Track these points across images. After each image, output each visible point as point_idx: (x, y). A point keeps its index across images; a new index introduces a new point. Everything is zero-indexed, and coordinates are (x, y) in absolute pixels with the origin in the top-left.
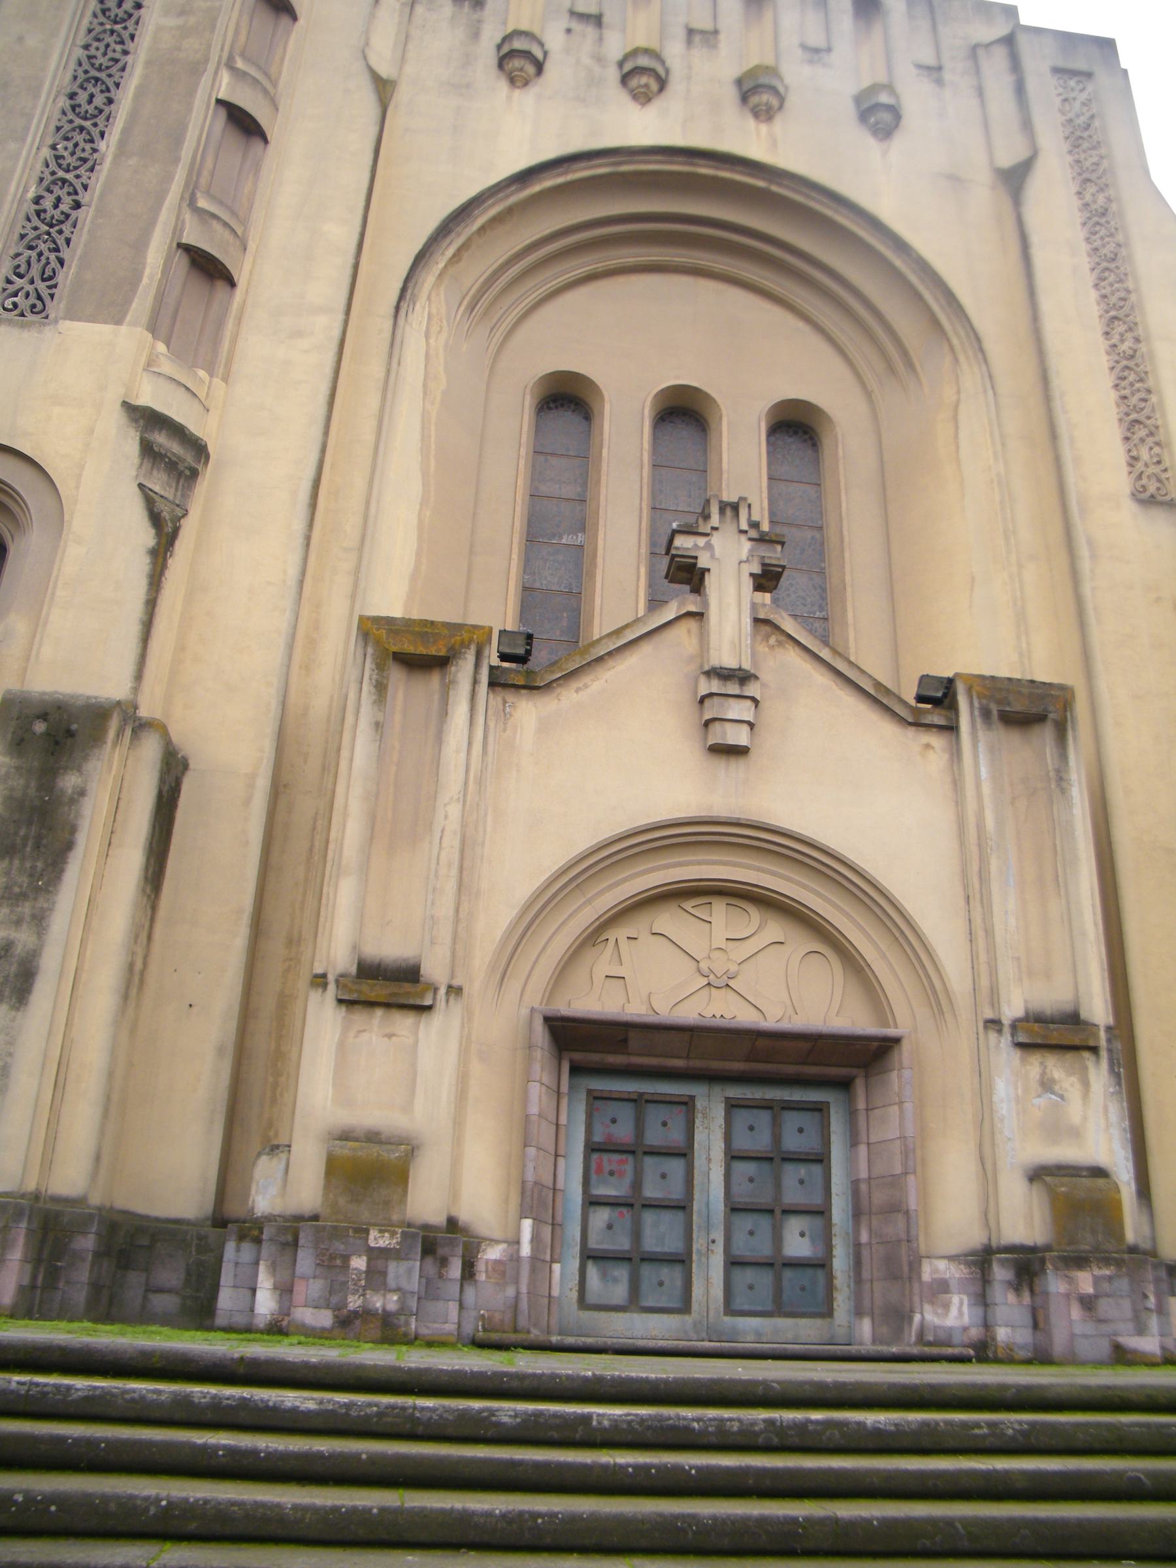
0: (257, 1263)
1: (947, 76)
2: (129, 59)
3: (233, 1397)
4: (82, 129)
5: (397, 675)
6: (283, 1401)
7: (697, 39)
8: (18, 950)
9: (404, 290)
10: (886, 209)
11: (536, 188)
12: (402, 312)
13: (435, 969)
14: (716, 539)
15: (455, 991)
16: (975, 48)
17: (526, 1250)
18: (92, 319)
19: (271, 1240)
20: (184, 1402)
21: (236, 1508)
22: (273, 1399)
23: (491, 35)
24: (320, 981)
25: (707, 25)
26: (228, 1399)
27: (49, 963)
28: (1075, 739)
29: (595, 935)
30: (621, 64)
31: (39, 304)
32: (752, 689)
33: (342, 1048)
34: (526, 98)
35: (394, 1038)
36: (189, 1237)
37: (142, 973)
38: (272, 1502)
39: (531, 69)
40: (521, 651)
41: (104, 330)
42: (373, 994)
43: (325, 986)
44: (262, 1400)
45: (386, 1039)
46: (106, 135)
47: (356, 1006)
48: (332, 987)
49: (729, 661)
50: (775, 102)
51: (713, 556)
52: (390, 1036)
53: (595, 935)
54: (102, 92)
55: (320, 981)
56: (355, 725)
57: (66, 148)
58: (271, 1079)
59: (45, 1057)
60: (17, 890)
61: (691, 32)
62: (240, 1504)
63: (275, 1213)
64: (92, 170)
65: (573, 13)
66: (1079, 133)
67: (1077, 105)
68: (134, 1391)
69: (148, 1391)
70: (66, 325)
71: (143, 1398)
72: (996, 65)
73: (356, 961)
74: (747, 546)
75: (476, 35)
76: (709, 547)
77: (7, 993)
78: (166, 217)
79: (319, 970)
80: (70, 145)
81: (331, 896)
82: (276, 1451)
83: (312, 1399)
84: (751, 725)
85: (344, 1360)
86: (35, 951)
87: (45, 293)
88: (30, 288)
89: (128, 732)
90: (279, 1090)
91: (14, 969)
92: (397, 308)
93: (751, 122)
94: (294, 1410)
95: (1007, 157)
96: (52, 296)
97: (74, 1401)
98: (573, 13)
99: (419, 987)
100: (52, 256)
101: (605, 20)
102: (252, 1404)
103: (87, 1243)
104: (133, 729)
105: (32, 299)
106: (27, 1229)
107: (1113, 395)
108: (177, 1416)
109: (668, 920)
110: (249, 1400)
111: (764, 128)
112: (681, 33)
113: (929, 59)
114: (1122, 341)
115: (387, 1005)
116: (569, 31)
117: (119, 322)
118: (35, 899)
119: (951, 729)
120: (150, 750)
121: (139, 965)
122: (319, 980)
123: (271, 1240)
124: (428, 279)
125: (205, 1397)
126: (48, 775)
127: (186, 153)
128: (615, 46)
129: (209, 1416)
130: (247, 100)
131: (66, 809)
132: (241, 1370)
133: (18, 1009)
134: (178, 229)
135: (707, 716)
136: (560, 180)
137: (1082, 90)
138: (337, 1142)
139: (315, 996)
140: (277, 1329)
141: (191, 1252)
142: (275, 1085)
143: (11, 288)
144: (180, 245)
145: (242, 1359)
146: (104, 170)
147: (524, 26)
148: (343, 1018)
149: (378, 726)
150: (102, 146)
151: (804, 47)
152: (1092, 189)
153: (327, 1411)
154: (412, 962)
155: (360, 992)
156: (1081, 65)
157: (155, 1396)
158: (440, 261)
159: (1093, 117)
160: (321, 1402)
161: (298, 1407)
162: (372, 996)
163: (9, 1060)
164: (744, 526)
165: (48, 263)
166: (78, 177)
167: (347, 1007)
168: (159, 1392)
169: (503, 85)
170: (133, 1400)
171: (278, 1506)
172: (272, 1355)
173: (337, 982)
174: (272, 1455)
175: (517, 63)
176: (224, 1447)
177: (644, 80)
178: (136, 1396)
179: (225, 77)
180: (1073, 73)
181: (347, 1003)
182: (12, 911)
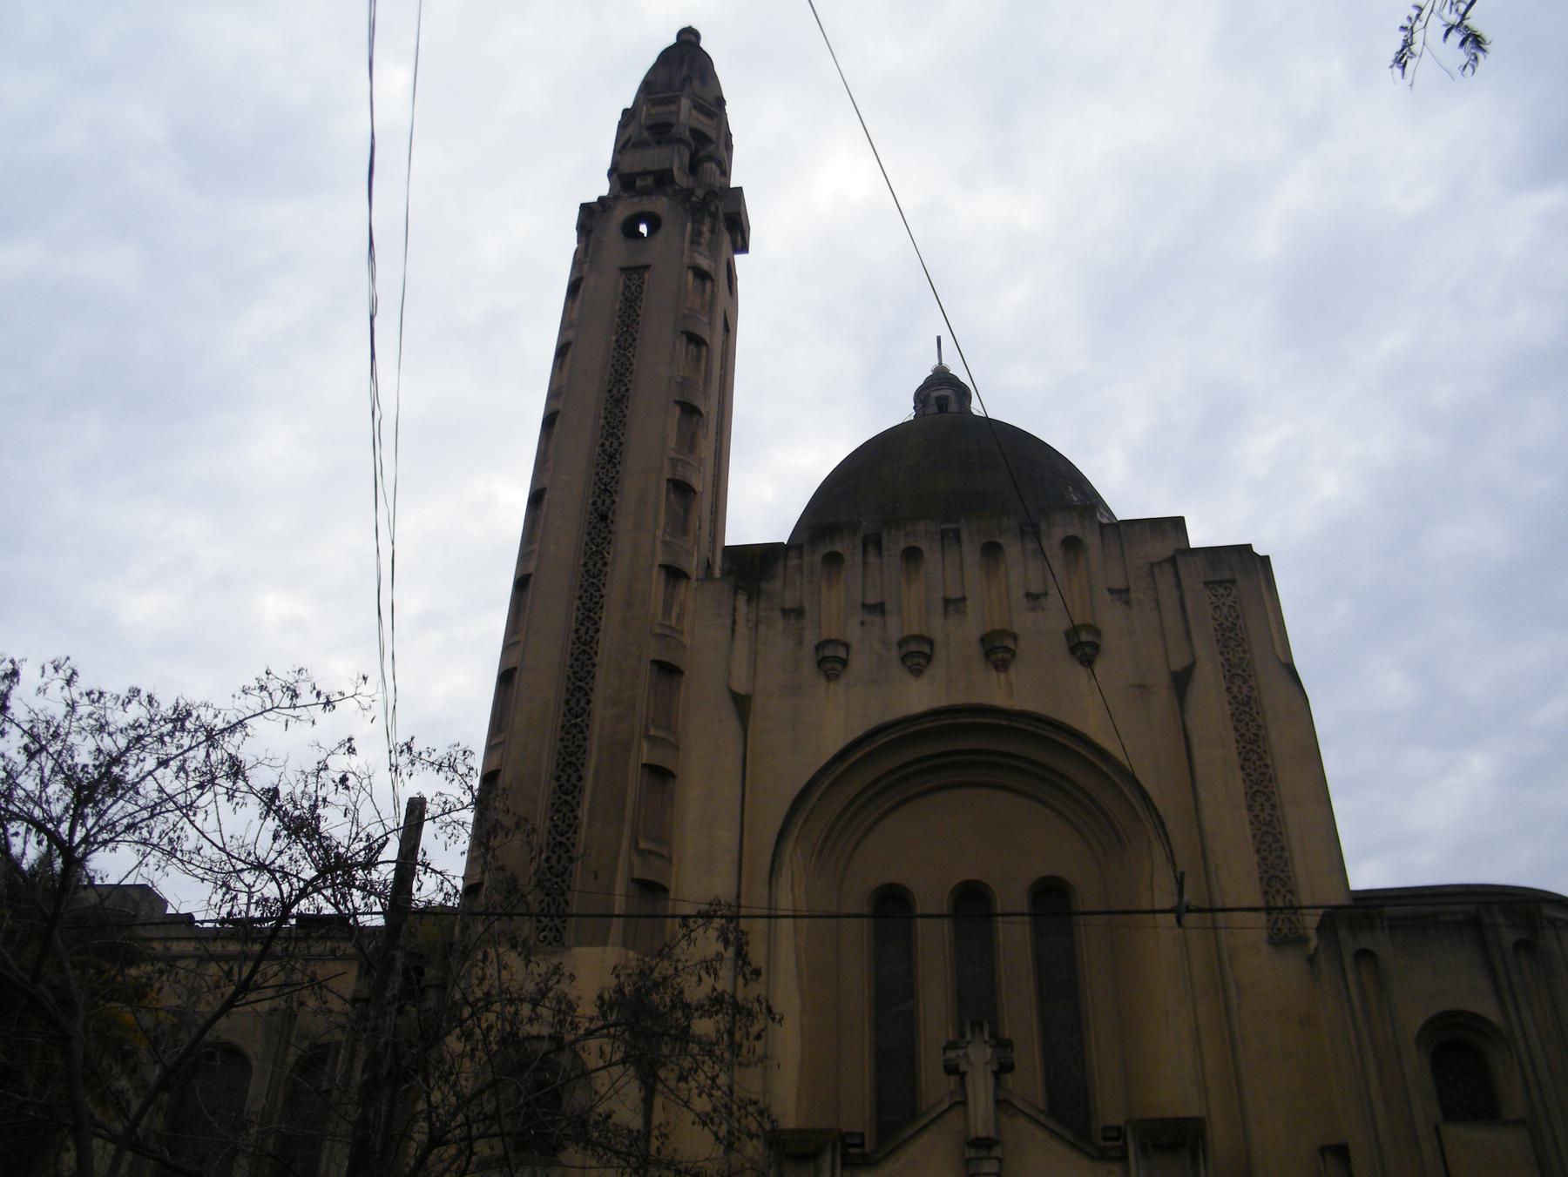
1: (1133, 595)
2: (587, 743)
4: (566, 802)
7: (951, 608)
9: (773, 862)
10: (1093, 725)
11: (852, 760)
12: (774, 880)
14: (970, 1050)
16: (1152, 565)
18: (590, 944)
23: (811, 638)
25: (959, 595)
28: (1205, 1156)
30: (900, 644)
32: (997, 1152)
39: (839, 667)
40: (858, 1141)
41: (599, 949)
46: (581, 805)
49: (981, 1131)
50: (1007, 656)
51: (968, 1062)
54: (575, 772)
57: (559, 819)
61: (947, 602)
64: (575, 832)
65: (865, 606)
66: (1227, 634)
67: (1225, 610)
70: (577, 950)
72: (1165, 580)
74: (989, 1051)
76: (966, 1055)
78: (622, 863)
80: (561, 815)
87: (560, 926)
92: (771, 877)
93: (994, 674)
95: (1178, 664)
96: (565, 928)
98: (865, 606)
101: (888, 607)
107: (1256, 858)
111: (1002, 676)
112: (939, 606)
113: (1119, 583)
114: (1262, 810)
116: (862, 623)
117: (605, 944)
119: (1124, 1158)
124: (788, 849)
127: (628, 813)
128: (895, 629)
130: (659, 759)
136: (868, 749)
137: (1228, 595)
144: (633, 880)
150: (579, 813)
151: (1028, 595)
152: (1238, 682)
156: (1226, 575)
159: (1238, 617)
164: (987, 1037)
165: (559, 905)
166: (568, 839)
169: (822, 681)
175: (829, 665)
177: (915, 660)
179: (645, 746)
180: (1220, 583)
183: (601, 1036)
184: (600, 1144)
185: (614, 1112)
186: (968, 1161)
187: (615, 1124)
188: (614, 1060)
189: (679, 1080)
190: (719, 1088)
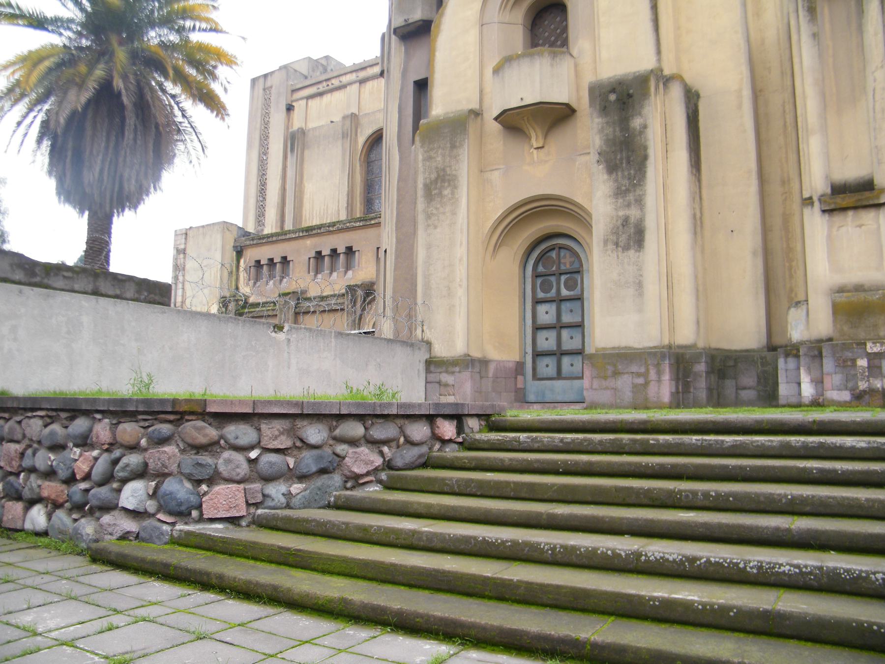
0: (798, 369)
3: (815, 442)
6: (845, 443)
8: (632, 220)
19: (805, 355)
20: (788, 445)
21: (832, 500)
22: (839, 442)
24: (808, 202)
26: (811, 443)
33: (829, 238)
35: (863, 227)
36: (755, 359)
37: (701, 218)
38: (853, 497)
42: (845, 203)
43: (812, 204)
44: (832, 443)
45: (858, 228)
47: (835, 213)
48: (817, 204)
52: (860, 226)
55: (808, 202)
56: (799, 40)
58: (787, 264)
59: (659, 272)
60: (624, 188)
62: (834, 498)
63: (804, 340)
68: (758, 441)
69: (765, 441)
71: (763, 444)
73: (830, 186)
77: (632, 244)
79: (806, 195)
81: (806, 149)
82: (848, 470)
83: (863, 441)
85: (874, 418)
86: (641, 219)
89: (661, 86)
90: (793, 270)
91: (632, 230)
94: (853, 448)
97: (727, 448)
99: (875, 193)
102: (827, 445)
103: (701, 367)
104: (663, 84)
106: (669, 364)
108: (784, 453)
110: (825, 443)
115: (855, 208)
118: (635, 191)
120: (676, 93)
121: (698, 215)
122: (808, 201)
123: (805, 355)
125: (798, 443)
126: (624, 122)
129: (802, 452)
131: (639, 138)
132: (815, 427)
133: (639, 251)
138: (837, 294)
139: (807, 211)
140: (816, 403)
141: (758, 366)
142: (790, 268)
145: (814, 421)
148: (828, 221)
153: (874, 447)
154: (867, 178)
155: (835, 203)
157: (770, 444)
160: (869, 443)
161: (855, 446)
162: (844, 204)
163: (641, 278)
167: (829, 214)
168: (772, 441)
170: (758, 446)
171: (857, 499)
172: (832, 418)
173: (820, 200)
174: (844, 472)
176: (816, 468)
178: (759, 444)
181: (828, 212)
182: (624, 200)
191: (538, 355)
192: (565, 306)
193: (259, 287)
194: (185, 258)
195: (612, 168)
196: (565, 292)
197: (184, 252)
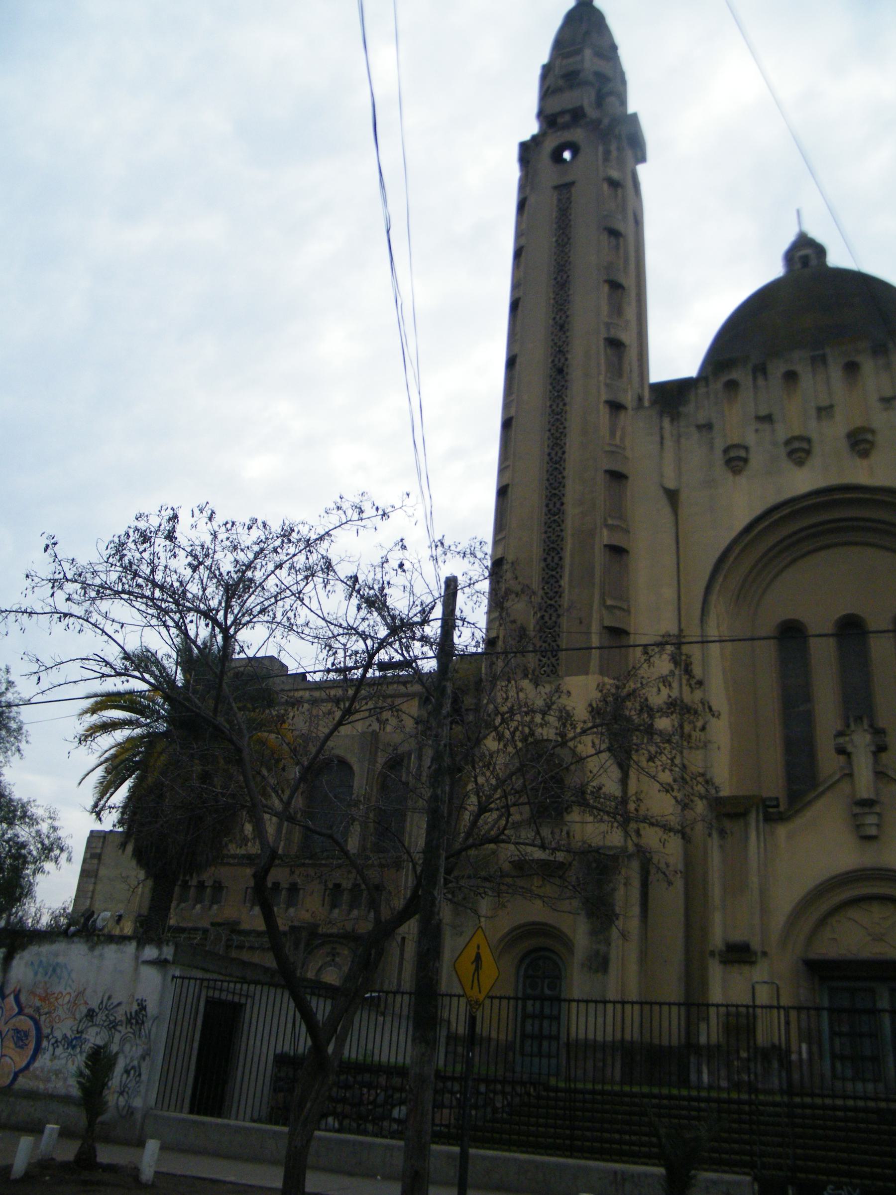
5: (727, 824)
13: (755, 945)
15: (765, 954)
17: (805, 1055)
18: (576, 675)
23: (719, 445)
24: (712, 954)
27: (614, 955)
29: (823, 921)
30: (788, 442)
31: (554, 669)
32: (877, 809)
34: (742, 480)
39: (741, 464)
40: (775, 803)
48: (717, 957)
50: (867, 446)
53: (823, 921)
55: (712, 954)
61: (820, 410)
64: (560, 597)
70: (567, 679)
75: (712, 448)
76: (852, 740)
78: (595, 616)
79: (711, 948)
80: (549, 586)
84: (878, 825)
88: (548, 662)
96: (558, 664)
100: (554, 644)
105: (551, 668)
109: (853, 913)
111: (865, 463)
112: (813, 413)
116: (757, 431)
117: (587, 673)
120: (635, 865)
124: (713, 598)
127: (597, 580)
134: (601, 619)
135: (858, 823)
140: (710, 1088)
143: (542, 664)
146: (566, 595)
147: (736, 442)
149: (721, 846)
150: (562, 583)
158: (717, 587)
164: (866, 727)
169: (730, 476)
175: (734, 464)
179: (605, 532)
183: (591, 734)
184: (596, 808)
185: (603, 785)
186: (855, 815)
187: (604, 794)
188: (602, 749)
189: (648, 761)
190: (676, 766)
191: (524, 1036)
192: (547, 1004)
193: (182, 909)
194: (99, 864)
195: (590, 915)
196: (547, 992)
197: (99, 857)
